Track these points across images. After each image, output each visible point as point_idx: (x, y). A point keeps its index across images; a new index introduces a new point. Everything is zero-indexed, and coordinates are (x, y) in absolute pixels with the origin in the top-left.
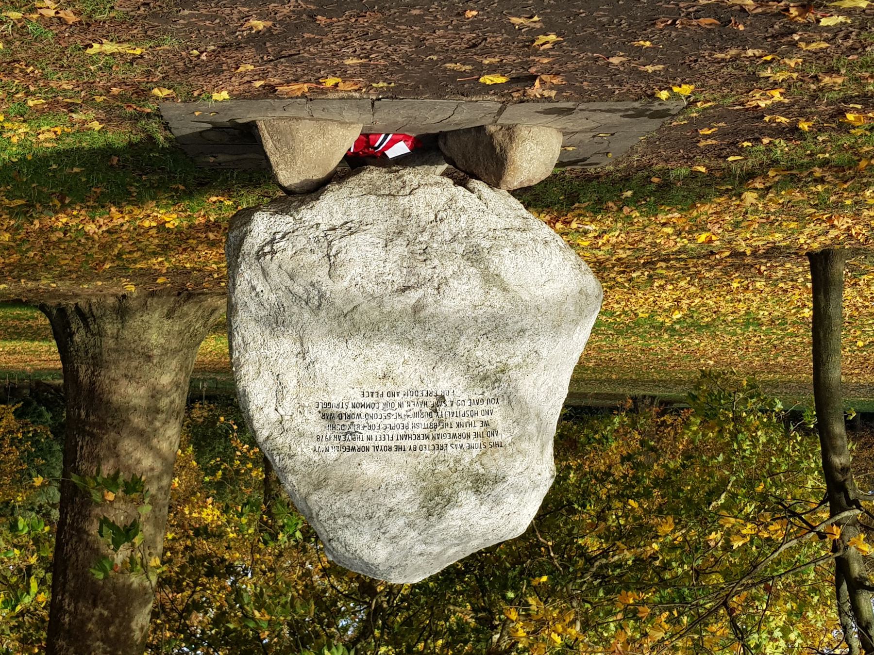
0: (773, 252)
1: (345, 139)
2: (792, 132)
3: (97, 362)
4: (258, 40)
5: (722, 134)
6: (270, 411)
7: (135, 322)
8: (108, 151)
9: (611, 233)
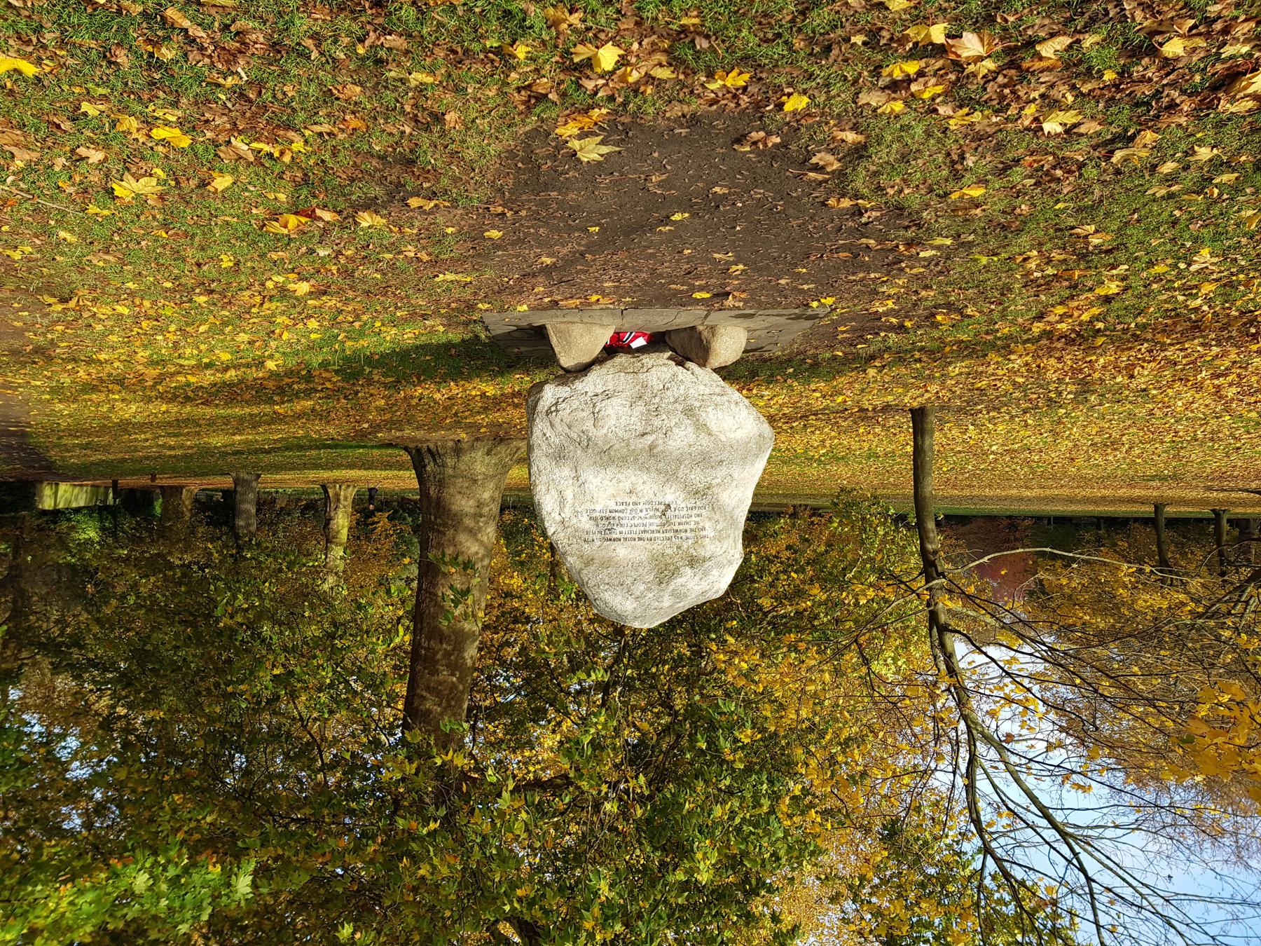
0: (886, 408)
1: (604, 336)
2: (901, 328)
3: (441, 484)
4: (547, 271)
5: (854, 330)
6: (555, 515)
7: (466, 458)
8: (449, 345)
9: (779, 397)
